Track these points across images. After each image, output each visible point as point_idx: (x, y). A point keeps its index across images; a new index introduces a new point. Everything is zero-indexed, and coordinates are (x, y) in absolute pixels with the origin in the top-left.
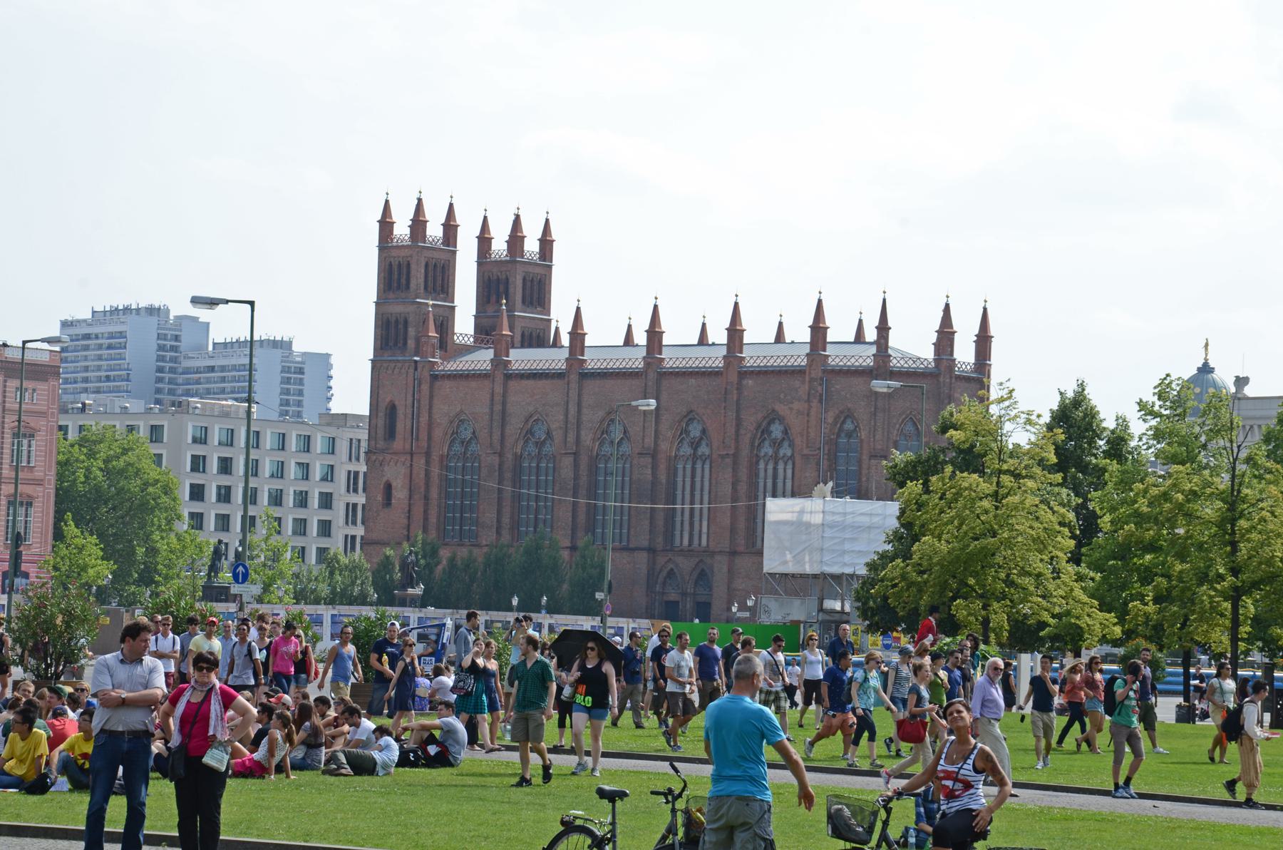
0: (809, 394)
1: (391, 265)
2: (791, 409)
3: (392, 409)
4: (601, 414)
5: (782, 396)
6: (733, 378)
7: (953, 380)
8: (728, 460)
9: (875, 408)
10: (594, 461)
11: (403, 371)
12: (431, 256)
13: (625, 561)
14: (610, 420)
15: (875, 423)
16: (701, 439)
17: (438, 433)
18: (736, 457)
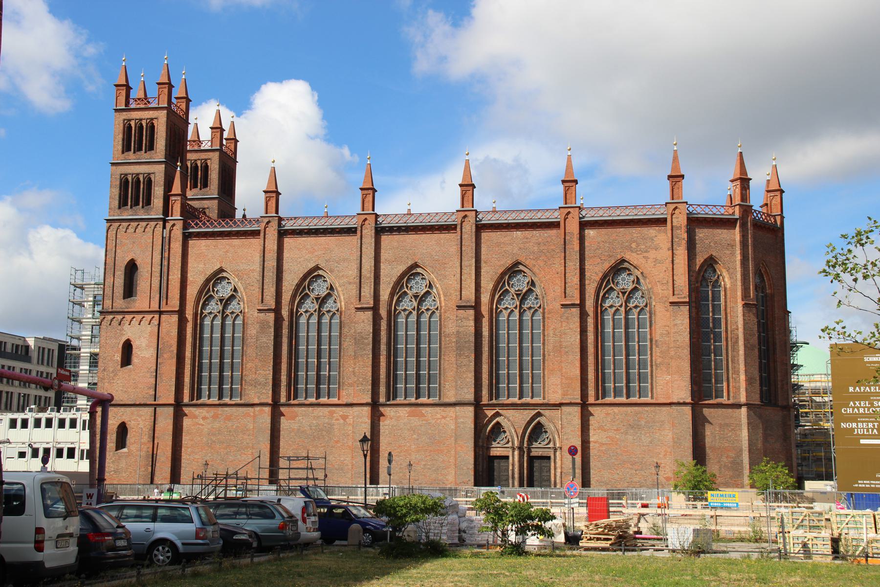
0: (672, 242)
1: (130, 127)
2: (646, 258)
3: (132, 268)
4: (402, 268)
5: (634, 245)
6: (573, 227)
8: (576, 311)
11: (149, 230)
13: (439, 416)
16: (530, 291)
17: (192, 292)
18: (582, 305)
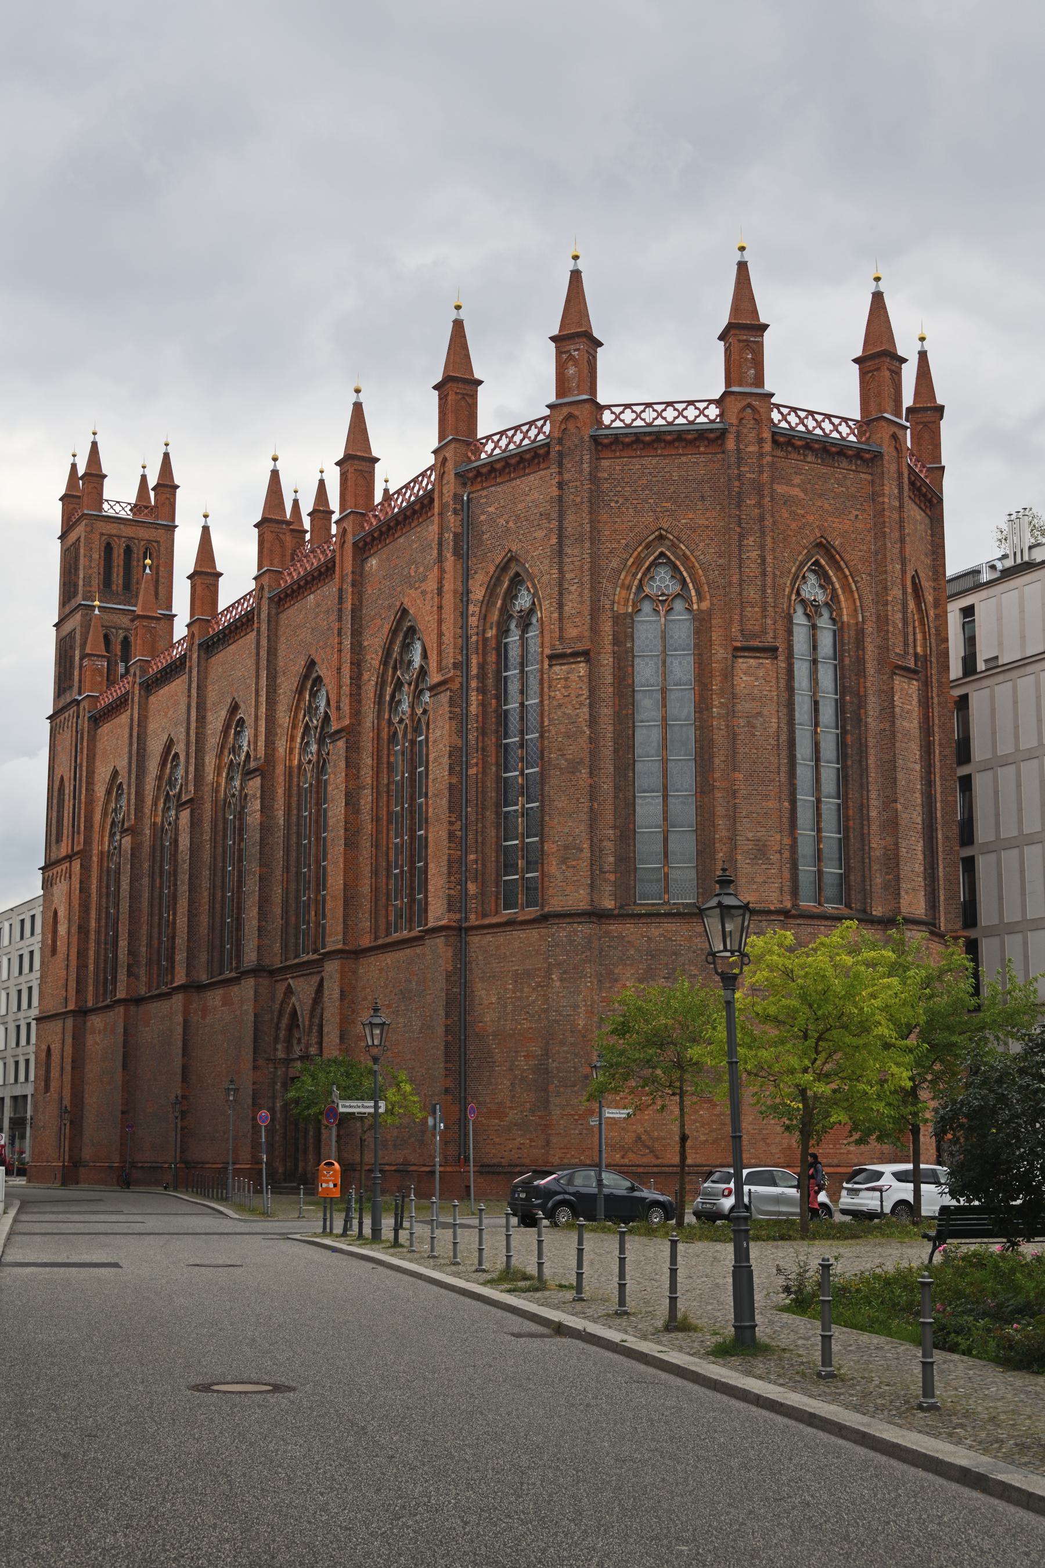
7: (768, 447)
9: (560, 537)
10: (221, 806)
12: (114, 532)
14: (237, 726)
15: (561, 571)
